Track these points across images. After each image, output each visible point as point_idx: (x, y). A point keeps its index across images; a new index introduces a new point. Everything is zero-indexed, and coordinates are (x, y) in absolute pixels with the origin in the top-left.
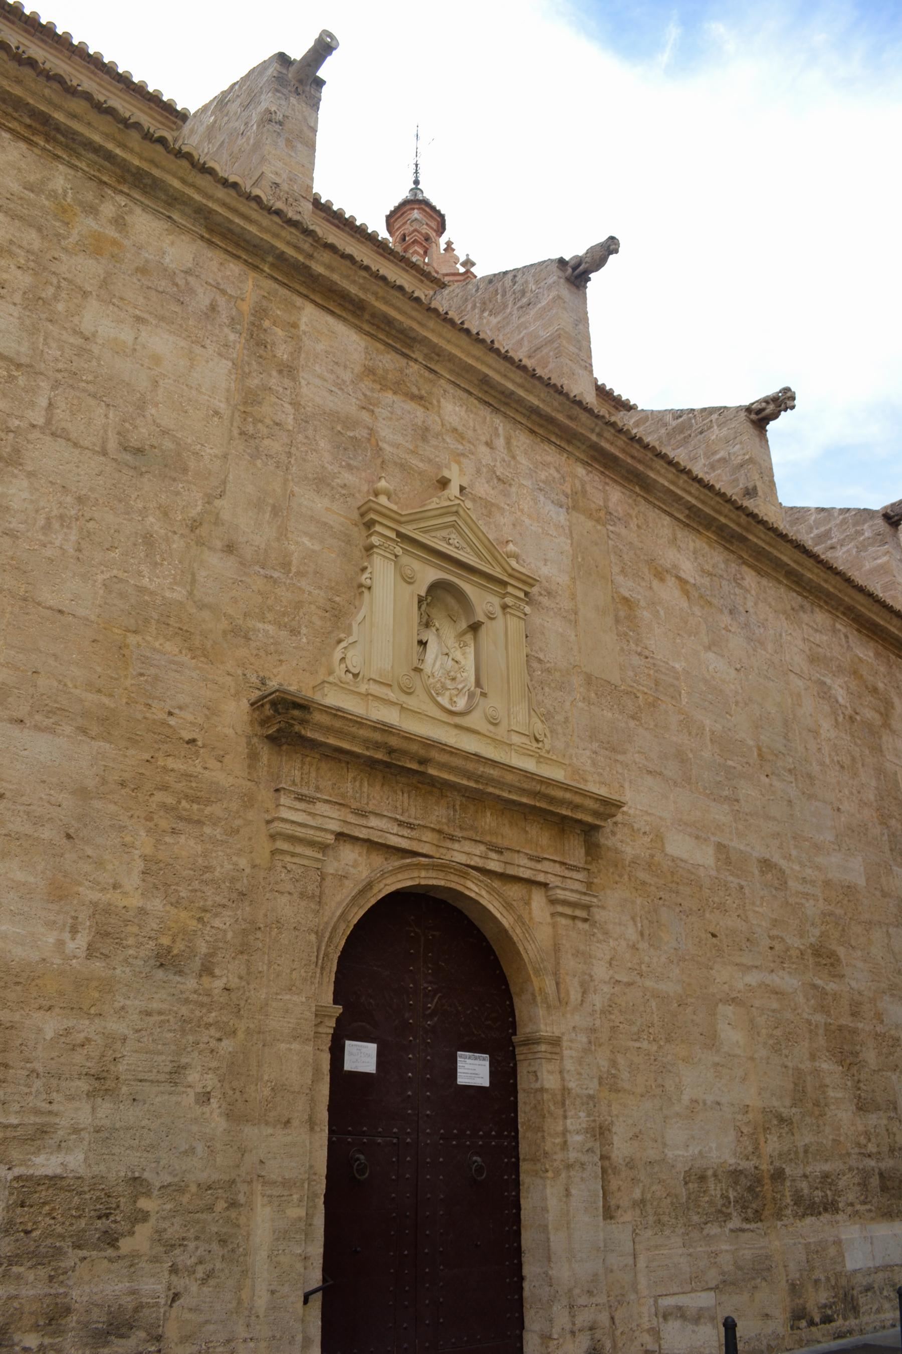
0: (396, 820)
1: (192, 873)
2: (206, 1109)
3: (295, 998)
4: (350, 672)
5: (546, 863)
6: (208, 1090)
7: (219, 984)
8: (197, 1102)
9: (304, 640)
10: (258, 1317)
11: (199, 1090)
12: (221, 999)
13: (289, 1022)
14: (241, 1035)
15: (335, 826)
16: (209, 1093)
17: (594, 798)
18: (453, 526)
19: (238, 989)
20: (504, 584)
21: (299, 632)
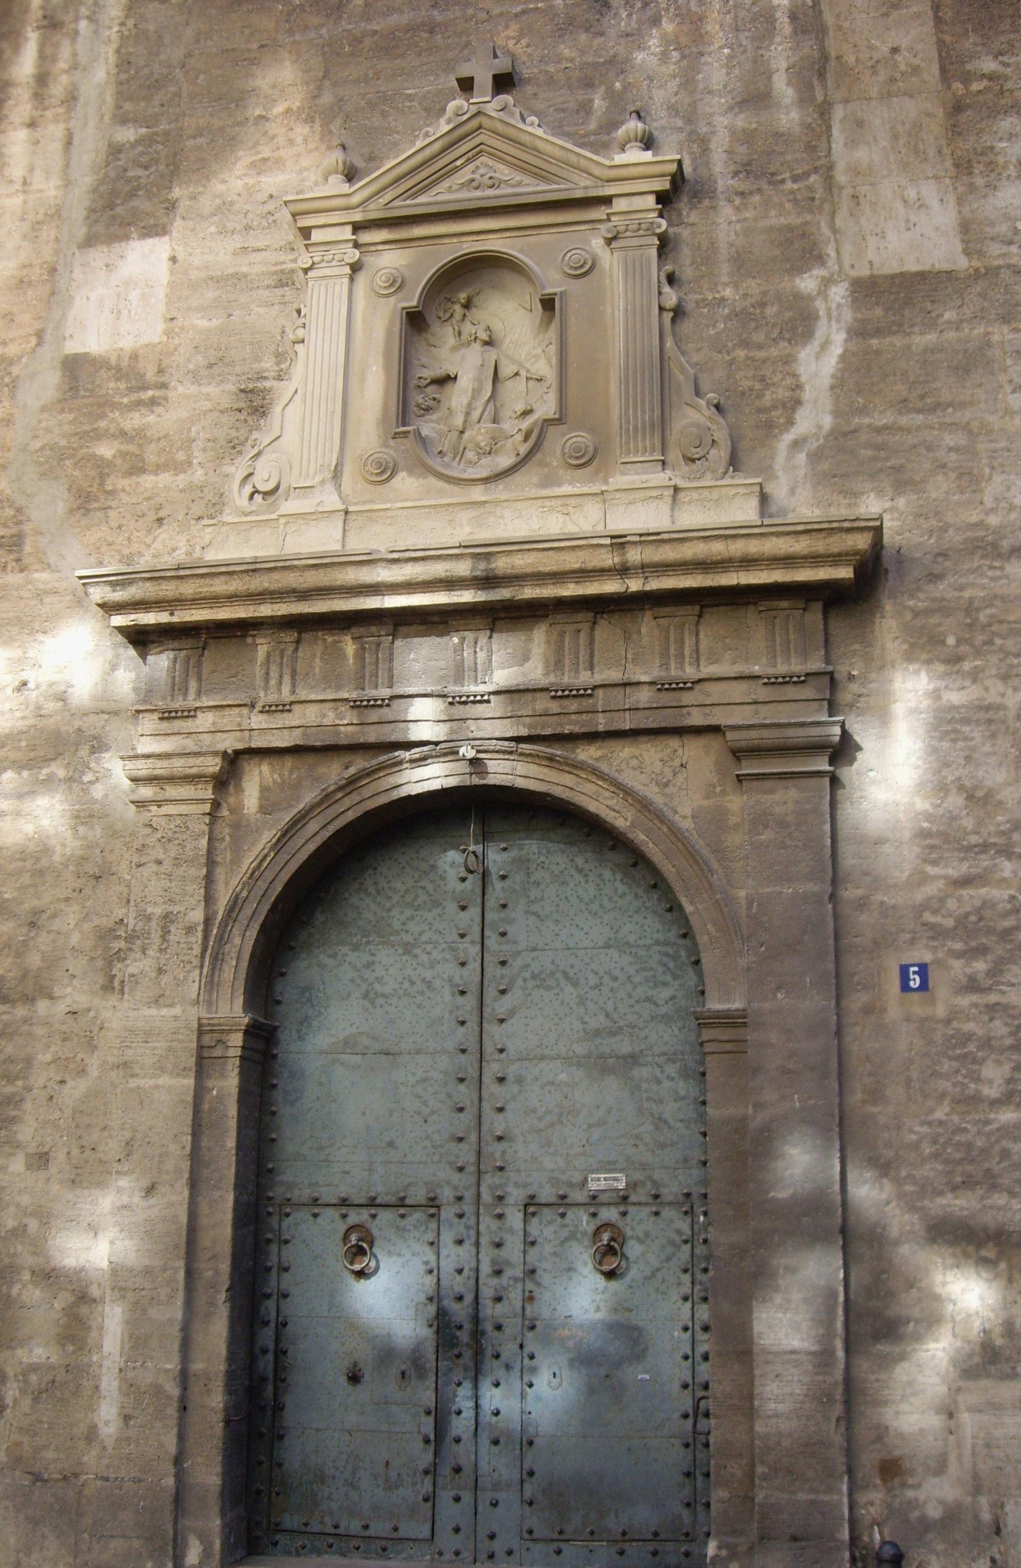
0: (346, 700)
1: (20, 864)
2: (42, 1175)
3: (164, 1011)
4: (257, 492)
5: (708, 686)
6: (45, 1150)
7: (61, 1008)
8: (29, 1167)
9: (200, 472)
10: (104, 1448)
11: (32, 1148)
12: (64, 1028)
13: (154, 1048)
14: (94, 1072)
15: (230, 743)
16: (47, 1153)
17: (789, 533)
18: (477, 152)
19: (89, 1010)
20: (607, 201)
21: (190, 464)
